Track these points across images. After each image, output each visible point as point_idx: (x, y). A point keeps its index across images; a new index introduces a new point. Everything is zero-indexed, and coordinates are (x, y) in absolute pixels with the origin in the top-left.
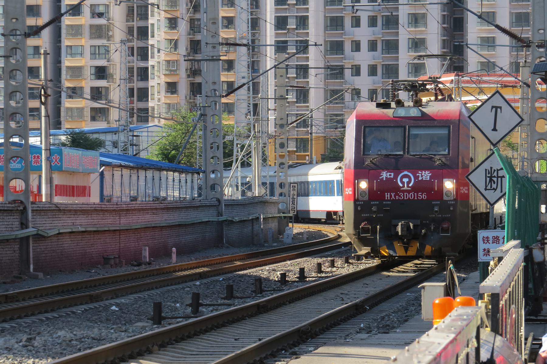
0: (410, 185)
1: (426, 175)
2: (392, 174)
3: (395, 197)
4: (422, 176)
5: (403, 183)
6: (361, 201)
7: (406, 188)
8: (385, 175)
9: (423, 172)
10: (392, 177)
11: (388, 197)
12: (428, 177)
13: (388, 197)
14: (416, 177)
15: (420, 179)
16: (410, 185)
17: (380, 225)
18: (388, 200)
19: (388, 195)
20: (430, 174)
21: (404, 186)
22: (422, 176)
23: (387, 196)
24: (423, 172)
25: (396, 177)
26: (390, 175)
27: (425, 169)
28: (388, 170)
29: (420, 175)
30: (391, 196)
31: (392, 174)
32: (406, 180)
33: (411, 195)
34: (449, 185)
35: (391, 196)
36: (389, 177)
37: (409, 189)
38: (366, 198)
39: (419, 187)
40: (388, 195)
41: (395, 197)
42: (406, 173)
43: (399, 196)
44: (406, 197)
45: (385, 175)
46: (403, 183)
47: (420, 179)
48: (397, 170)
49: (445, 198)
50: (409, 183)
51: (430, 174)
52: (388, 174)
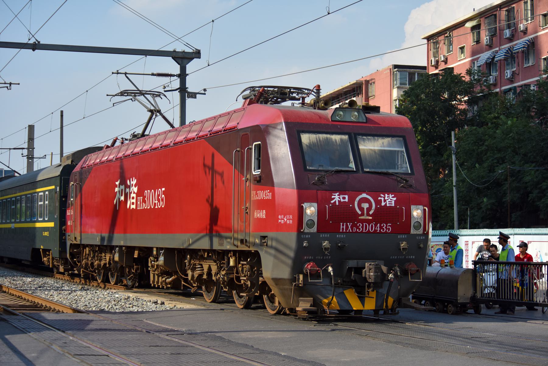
0: (371, 213)
1: (389, 200)
2: (347, 197)
3: (352, 229)
4: (385, 201)
6: (308, 234)
7: (365, 217)
9: (386, 195)
10: (347, 200)
11: (343, 229)
12: (393, 201)
13: (343, 229)
15: (383, 204)
16: (371, 213)
17: (332, 267)
18: (343, 232)
19: (343, 225)
20: (395, 199)
21: (363, 214)
22: (385, 201)
23: (342, 227)
24: (386, 195)
25: (352, 200)
26: (344, 198)
29: (383, 199)
32: (365, 206)
33: (372, 225)
36: (342, 200)
37: (371, 218)
38: (314, 229)
39: (382, 214)
40: (343, 225)
42: (364, 195)
43: (358, 228)
44: (366, 230)
46: (362, 209)
47: (383, 204)
48: (354, 191)
49: (413, 231)
50: (369, 209)
51: (395, 199)
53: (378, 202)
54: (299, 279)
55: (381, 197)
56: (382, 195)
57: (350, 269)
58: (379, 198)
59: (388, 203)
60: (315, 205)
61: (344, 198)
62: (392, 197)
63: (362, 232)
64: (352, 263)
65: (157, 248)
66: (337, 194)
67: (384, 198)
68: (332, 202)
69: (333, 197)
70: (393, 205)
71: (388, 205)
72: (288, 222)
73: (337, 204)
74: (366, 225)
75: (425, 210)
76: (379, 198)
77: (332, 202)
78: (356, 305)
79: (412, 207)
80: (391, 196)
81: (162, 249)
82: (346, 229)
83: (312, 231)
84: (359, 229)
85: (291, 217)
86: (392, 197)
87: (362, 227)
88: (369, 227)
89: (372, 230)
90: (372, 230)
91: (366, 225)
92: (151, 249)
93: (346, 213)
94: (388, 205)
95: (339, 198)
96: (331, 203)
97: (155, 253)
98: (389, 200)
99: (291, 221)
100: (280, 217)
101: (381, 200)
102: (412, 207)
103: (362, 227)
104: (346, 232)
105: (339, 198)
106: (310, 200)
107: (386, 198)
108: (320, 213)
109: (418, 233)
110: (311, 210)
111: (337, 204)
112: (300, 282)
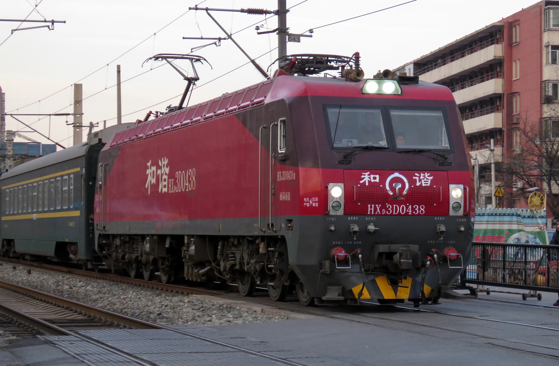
1: (425, 180)
2: (377, 176)
3: (381, 212)
4: (420, 180)
5: (393, 189)
8: (367, 178)
10: (377, 180)
11: (371, 211)
12: (429, 181)
13: (371, 211)
14: (412, 182)
15: (418, 184)
18: (371, 215)
19: (371, 207)
20: (431, 178)
22: (420, 180)
23: (370, 208)
24: (422, 175)
25: (383, 180)
26: (375, 178)
27: (424, 171)
28: (373, 171)
29: (417, 178)
30: (375, 209)
31: (377, 176)
34: (456, 193)
35: (375, 209)
36: (373, 181)
37: (403, 198)
38: (341, 212)
39: (416, 196)
40: (371, 207)
41: (381, 212)
42: (396, 175)
43: (387, 210)
45: (367, 178)
46: (393, 189)
47: (418, 184)
49: (452, 213)
51: (431, 178)
52: (372, 176)
53: (412, 182)
54: (325, 265)
55: (416, 176)
56: (416, 174)
57: (381, 254)
58: (414, 178)
59: (423, 183)
60: (342, 185)
61: (375, 178)
62: (428, 176)
63: (392, 214)
64: (383, 248)
65: (188, 236)
66: (367, 174)
67: (419, 177)
68: (361, 182)
69: (363, 176)
70: (429, 185)
71: (424, 185)
72: (314, 205)
73: (367, 184)
74: (396, 207)
75: (465, 189)
76: (414, 178)
77: (361, 182)
78: (388, 293)
79: (451, 186)
80: (426, 175)
81: (193, 236)
82: (375, 212)
83: (338, 214)
84: (389, 211)
85: (317, 199)
86: (428, 176)
87: (392, 209)
88: (400, 209)
89: (403, 211)
90: (403, 211)
91: (396, 207)
92: (182, 237)
93: (376, 195)
94: (424, 185)
95: (370, 178)
96: (360, 184)
97: (186, 241)
98: (425, 180)
99: (317, 205)
100: (305, 199)
101: (416, 180)
102: (451, 186)
103: (392, 209)
104: (374, 215)
105: (370, 178)
106: (336, 181)
107: (422, 178)
108: (347, 195)
109: (458, 215)
110: (336, 192)
111: (367, 184)
112: (327, 269)
